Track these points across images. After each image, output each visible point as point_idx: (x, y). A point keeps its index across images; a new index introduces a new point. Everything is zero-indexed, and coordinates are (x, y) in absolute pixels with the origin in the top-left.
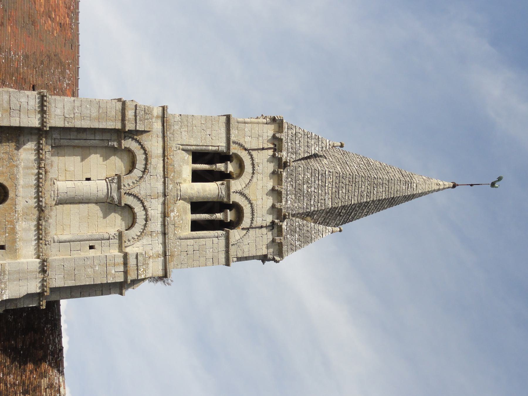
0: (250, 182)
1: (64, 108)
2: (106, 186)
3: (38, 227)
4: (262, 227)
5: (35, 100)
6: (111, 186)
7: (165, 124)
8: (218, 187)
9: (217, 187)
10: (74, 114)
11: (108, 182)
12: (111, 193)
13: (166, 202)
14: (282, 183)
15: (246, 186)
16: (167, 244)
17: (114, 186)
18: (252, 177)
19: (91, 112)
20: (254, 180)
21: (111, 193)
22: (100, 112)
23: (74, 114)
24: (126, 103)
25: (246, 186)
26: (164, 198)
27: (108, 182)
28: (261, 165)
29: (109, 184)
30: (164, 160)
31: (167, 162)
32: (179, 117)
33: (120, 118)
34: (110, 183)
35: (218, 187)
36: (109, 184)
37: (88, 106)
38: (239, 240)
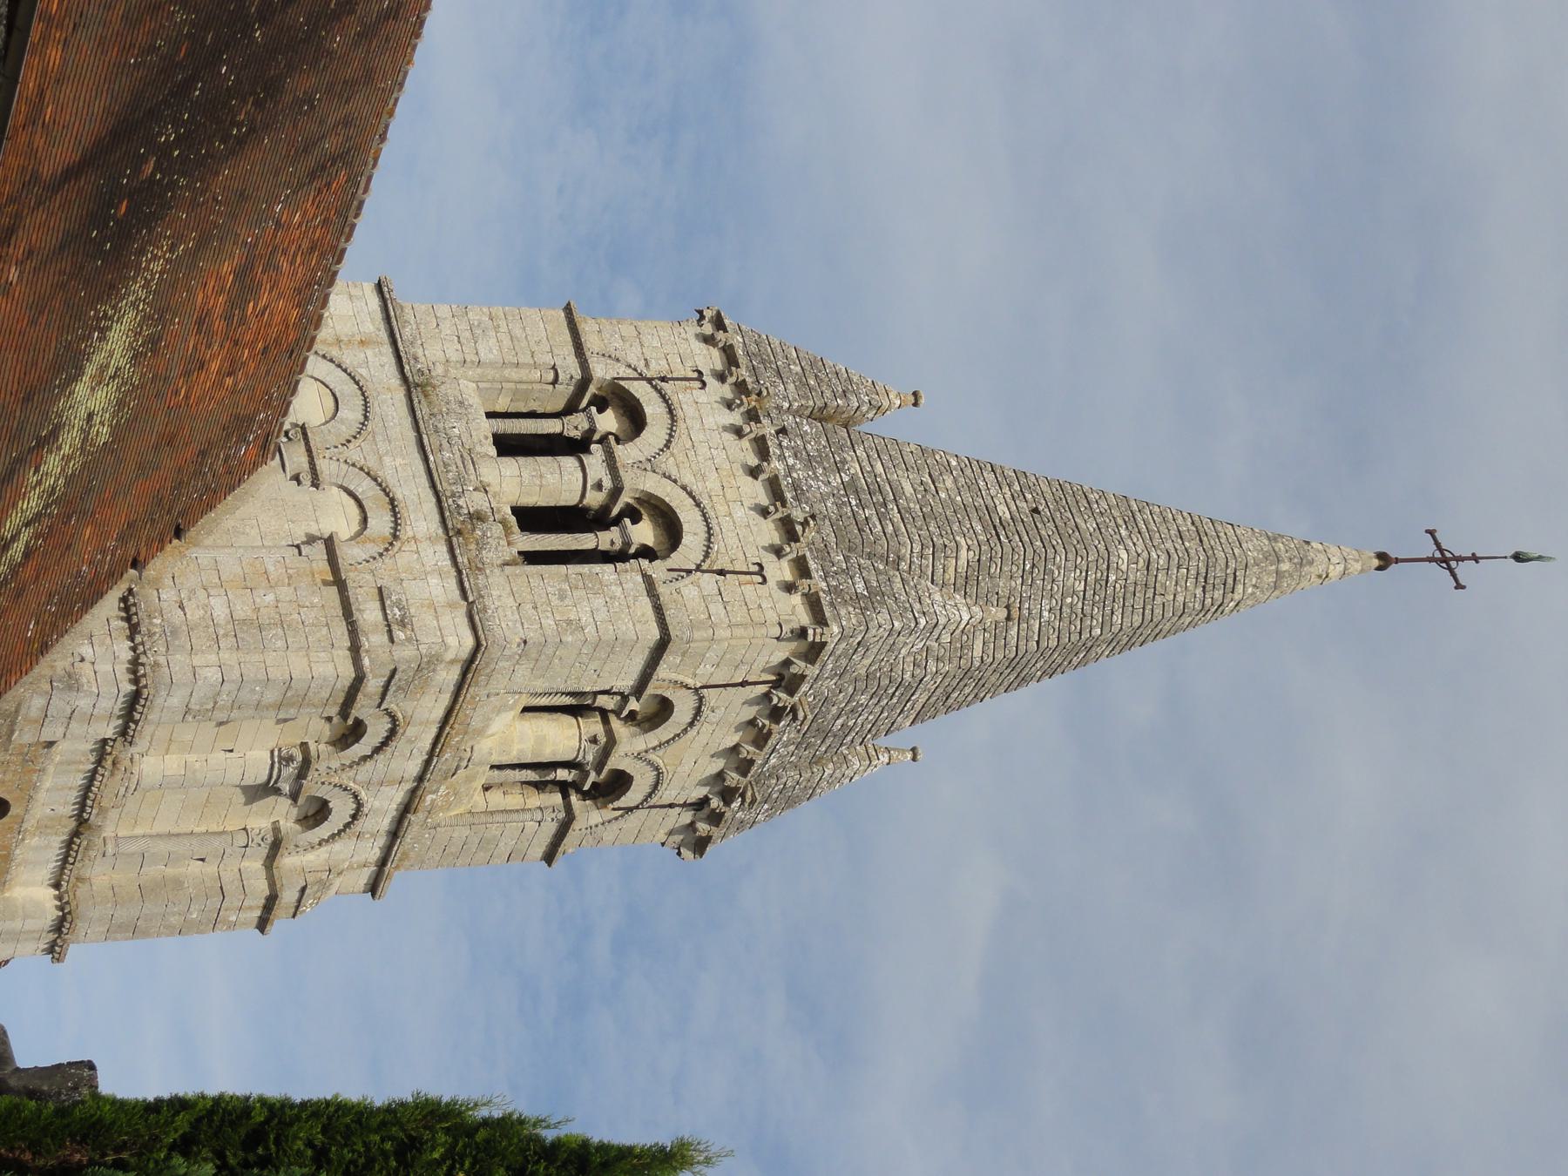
0: (673, 739)
2: (268, 767)
3: (69, 844)
4: (671, 806)
6: (280, 770)
7: (470, 676)
8: (580, 748)
9: (578, 744)
11: (276, 760)
12: (276, 782)
13: (420, 793)
14: (764, 746)
15: (660, 746)
16: (394, 852)
17: (291, 770)
18: (686, 730)
20: (692, 733)
21: (276, 782)
23: (216, 703)
24: (365, 681)
25: (660, 746)
26: (416, 784)
27: (276, 760)
28: (720, 712)
29: (277, 765)
31: (448, 733)
32: (519, 645)
34: (280, 763)
35: (580, 748)
36: (277, 765)
38: (597, 826)
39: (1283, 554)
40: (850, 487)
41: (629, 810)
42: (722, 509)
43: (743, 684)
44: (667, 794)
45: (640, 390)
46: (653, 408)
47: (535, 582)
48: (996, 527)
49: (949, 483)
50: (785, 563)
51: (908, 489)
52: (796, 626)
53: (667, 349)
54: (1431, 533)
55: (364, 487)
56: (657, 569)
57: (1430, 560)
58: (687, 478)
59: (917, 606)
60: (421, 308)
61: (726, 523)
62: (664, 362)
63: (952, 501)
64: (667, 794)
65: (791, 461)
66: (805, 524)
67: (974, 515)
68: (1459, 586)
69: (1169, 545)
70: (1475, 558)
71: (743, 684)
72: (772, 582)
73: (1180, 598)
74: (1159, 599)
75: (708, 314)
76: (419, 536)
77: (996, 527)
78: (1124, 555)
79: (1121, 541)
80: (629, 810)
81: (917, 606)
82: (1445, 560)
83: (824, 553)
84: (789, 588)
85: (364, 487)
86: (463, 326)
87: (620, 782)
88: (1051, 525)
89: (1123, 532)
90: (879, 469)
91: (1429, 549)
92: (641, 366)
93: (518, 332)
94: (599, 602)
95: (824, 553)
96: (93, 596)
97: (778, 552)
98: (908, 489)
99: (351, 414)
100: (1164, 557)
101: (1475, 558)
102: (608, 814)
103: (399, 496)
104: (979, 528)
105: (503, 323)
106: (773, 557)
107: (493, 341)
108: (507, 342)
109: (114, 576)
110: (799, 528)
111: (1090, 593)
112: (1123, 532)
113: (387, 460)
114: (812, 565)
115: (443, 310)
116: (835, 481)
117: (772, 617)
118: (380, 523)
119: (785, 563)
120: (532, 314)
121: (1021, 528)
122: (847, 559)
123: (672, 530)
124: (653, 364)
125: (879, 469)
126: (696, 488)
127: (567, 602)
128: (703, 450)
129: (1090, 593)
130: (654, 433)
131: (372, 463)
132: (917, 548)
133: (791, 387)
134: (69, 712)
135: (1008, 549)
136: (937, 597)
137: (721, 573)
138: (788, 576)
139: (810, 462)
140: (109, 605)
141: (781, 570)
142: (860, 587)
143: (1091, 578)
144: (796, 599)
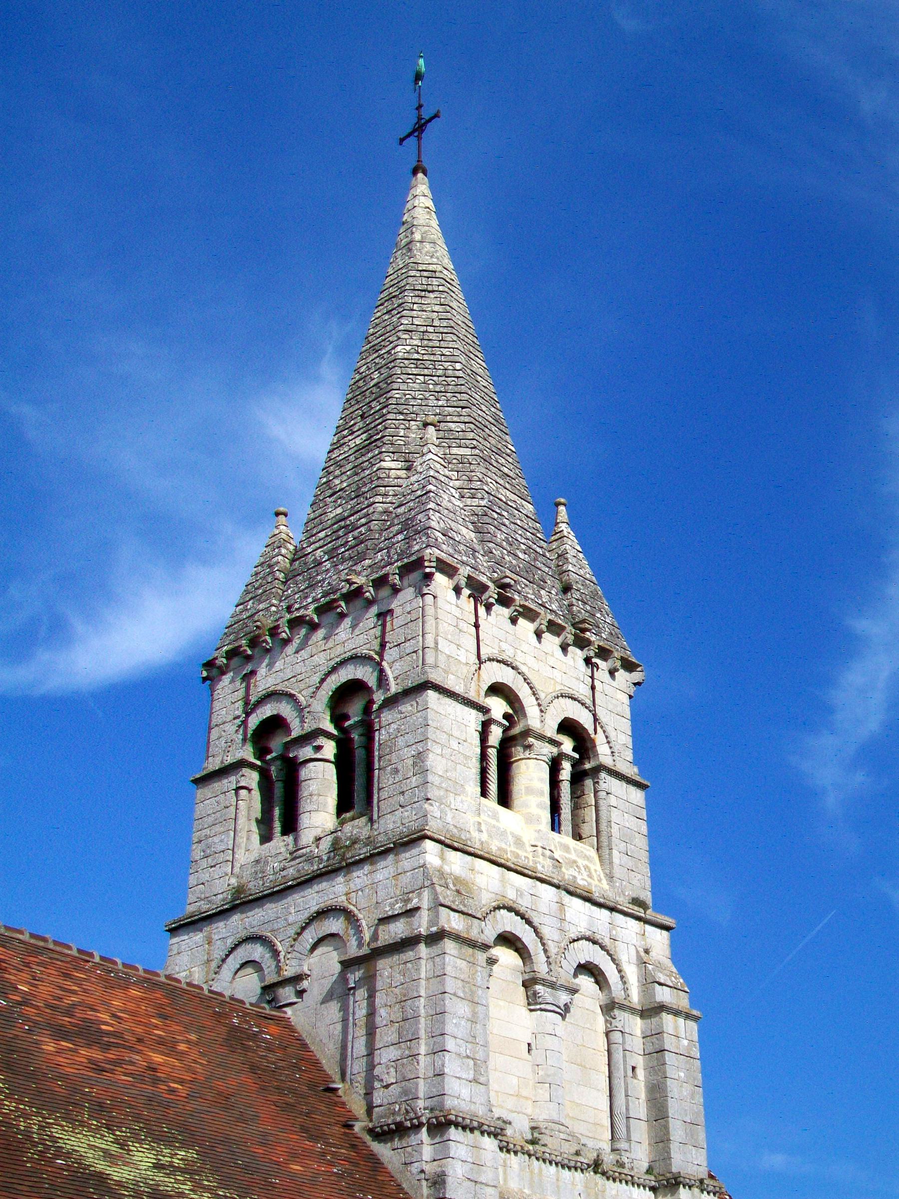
0: (528, 684)
1: (459, 1078)
4: (593, 688)
5: (458, 1144)
10: (468, 1057)
12: (559, 1007)
19: (463, 1017)
20: (523, 669)
21: (559, 1007)
22: (462, 995)
23: (468, 1057)
28: (504, 646)
30: (509, 869)
33: (470, 950)
35: (536, 759)
37: (454, 1021)
41: (596, 720)
42: (339, 650)
43: (477, 626)
44: (583, 691)
45: (254, 721)
46: (267, 711)
47: (384, 794)
49: (337, 481)
53: (228, 703)
54: (402, 140)
55: (310, 937)
56: (379, 697)
58: (316, 679)
59: (419, 493)
60: (191, 898)
61: (350, 645)
62: (237, 705)
64: (583, 691)
65: (310, 600)
69: (395, 319)
71: (477, 626)
73: (437, 308)
74: (436, 323)
75: (205, 674)
76: (345, 890)
79: (389, 352)
80: (596, 720)
82: (419, 128)
85: (310, 937)
86: (204, 863)
87: (568, 727)
88: (373, 404)
91: (412, 141)
92: (238, 722)
93: (210, 820)
94: (401, 742)
96: (375, 1162)
99: (257, 952)
101: (420, 107)
102: (599, 739)
103: (315, 909)
105: (204, 832)
107: (216, 839)
108: (218, 828)
109: (355, 1144)
111: (426, 372)
113: (291, 919)
115: (192, 880)
116: (328, 565)
118: (335, 925)
120: (199, 810)
122: (381, 550)
123: (354, 688)
124: (238, 713)
126: (325, 669)
127: (400, 767)
128: (299, 668)
129: (426, 372)
130: (285, 710)
131: (292, 931)
132: (379, 499)
133: (261, 606)
134: (470, 1183)
137: (383, 645)
139: (312, 586)
140: (383, 1150)
143: (415, 371)
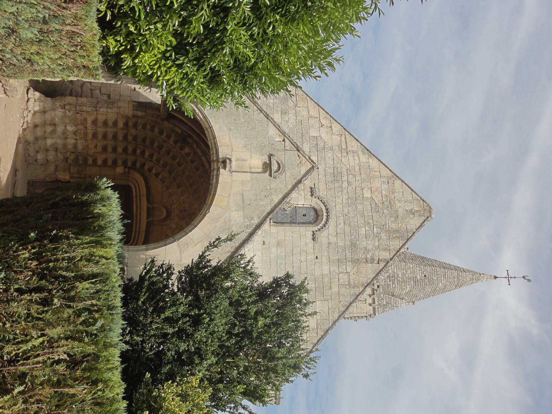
39: (475, 279)
40: (389, 277)
48: (416, 281)
50: (371, 298)
51: (400, 275)
52: (369, 314)
54: (507, 271)
57: (505, 278)
59: (395, 305)
63: (409, 276)
66: (377, 291)
67: (412, 280)
68: (509, 284)
70: (515, 278)
72: (367, 303)
77: (416, 281)
78: (441, 284)
81: (395, 305)
82: (508, 278)
83: (379, 296)
84: (370, 305)
89: (442, 279)
90: (395, 271)
95: (379, 296)
97: (370, 296)
98: (400, 275)
100: (449, 284)
101: (515, 278)
104: (412, 283)
106: (369, 297)
110: (375, 292)
112: (442, 279)
114: (376, 299)
117: (365, 311)
119: (371, 299)
121: (421, 281)
122: (383, 295)
125: (395, 271)
135: (417, 287)
136: (400, 302)
138: (371, 302)
141: (370, 300)
142: (385, 302)
144: (371, 307)
